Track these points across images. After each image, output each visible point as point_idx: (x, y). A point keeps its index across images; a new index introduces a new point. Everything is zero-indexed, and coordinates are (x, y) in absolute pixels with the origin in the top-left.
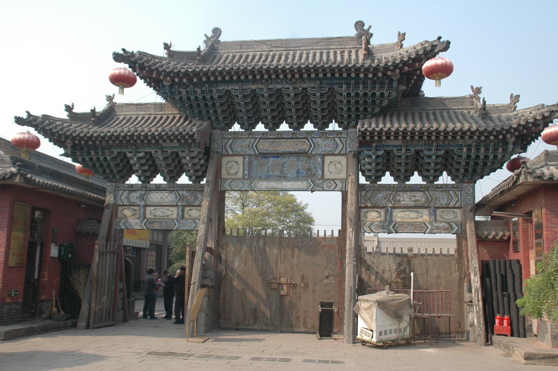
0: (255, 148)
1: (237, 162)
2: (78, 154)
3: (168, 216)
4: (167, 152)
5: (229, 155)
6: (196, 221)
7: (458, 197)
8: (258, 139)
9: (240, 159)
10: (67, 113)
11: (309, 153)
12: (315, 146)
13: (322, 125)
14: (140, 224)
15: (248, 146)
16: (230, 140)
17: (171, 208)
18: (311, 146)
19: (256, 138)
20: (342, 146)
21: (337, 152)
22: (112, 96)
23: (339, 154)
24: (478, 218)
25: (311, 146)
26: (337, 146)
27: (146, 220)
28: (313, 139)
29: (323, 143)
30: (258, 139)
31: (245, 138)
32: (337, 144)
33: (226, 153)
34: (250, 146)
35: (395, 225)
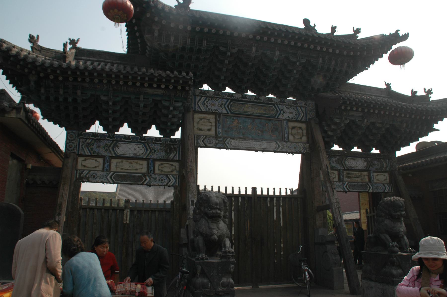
0: (227, 108)
1: (209, 120)
2: (43, 90)
3: (136, 170)
4: (148, 99)
5: (201, 112)
6: (168, 176)
8: (230, 100)
9: (212, 118)
10: (31, 44)
11: (276, 117)
13: (282, 95)
15: (221, 106)
16: (203, 98)
17: (141, 162)
18: (277, 112)
19: (228, 99)
20: (303, 114)
22: (76, 40)
23: (301, 122)
25: (277, 112)
26: (299, 114)
27: (112, 173)
29: (288, 111)
30: (230, 100)
31: (218, 98)
32: (298, 112)
33: (199, 110)
34: (223, 106)
35: (347, 185)
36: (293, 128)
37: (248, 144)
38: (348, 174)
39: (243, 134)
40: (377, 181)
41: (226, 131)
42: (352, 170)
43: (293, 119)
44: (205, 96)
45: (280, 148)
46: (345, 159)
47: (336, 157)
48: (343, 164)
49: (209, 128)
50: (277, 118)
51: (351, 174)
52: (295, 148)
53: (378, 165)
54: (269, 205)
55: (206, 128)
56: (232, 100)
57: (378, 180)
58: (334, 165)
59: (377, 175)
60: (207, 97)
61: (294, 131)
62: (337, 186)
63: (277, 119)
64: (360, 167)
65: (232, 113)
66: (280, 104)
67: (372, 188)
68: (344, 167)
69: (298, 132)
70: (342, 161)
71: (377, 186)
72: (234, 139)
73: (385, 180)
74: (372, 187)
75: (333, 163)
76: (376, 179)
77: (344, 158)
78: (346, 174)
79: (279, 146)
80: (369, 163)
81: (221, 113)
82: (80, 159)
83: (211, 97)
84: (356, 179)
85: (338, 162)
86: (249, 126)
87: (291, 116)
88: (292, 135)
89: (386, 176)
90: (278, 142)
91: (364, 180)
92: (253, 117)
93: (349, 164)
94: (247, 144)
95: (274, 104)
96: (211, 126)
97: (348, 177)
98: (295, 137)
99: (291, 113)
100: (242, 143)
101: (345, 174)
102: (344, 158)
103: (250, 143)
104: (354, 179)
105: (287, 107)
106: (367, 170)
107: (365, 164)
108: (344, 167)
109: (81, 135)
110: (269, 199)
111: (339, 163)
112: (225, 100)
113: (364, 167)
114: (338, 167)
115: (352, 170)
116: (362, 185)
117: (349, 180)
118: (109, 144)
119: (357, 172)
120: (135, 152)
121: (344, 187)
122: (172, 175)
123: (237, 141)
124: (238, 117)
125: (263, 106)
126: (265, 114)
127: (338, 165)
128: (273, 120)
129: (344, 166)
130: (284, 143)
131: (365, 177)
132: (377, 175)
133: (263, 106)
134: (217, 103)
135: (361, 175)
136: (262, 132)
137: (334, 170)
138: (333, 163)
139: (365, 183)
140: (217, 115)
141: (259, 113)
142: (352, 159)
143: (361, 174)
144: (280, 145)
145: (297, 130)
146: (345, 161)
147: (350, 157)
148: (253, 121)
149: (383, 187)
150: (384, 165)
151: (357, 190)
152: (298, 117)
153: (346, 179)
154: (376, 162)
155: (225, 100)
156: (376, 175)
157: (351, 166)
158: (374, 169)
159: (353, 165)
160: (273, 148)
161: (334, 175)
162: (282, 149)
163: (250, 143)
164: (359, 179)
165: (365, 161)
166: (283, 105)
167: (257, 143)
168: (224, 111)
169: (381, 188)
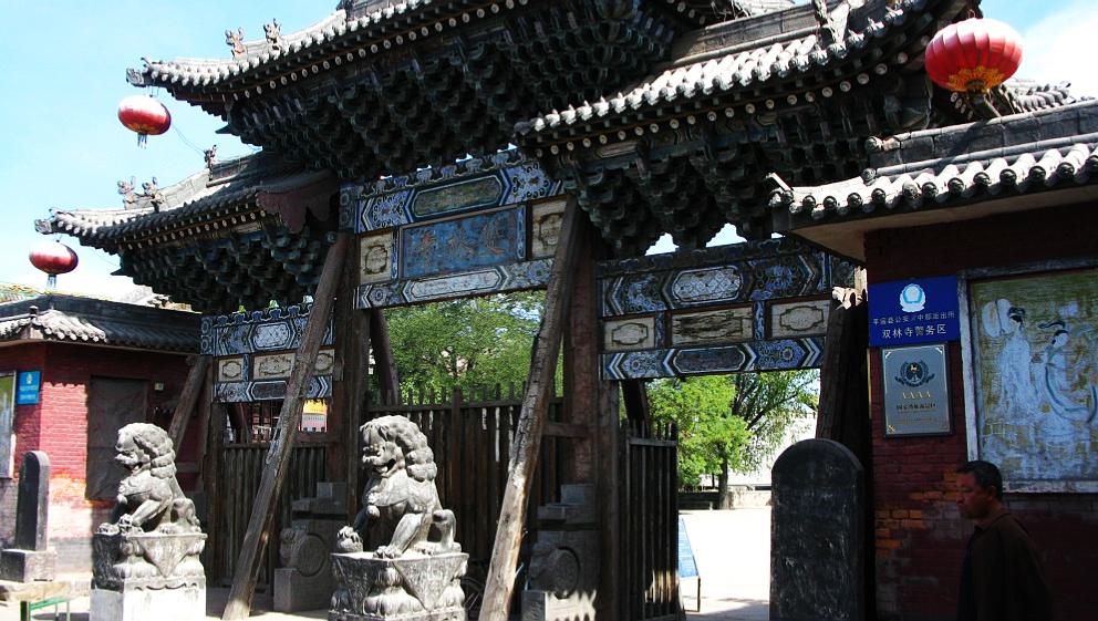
7: (820, 270)
9: (387, 239)
12: (511, 186)
14: (657, 364)
15: (398, 210)
18: (504, 187)
19: (411, 189)
21: (553, 193)
24: (29, 382)
25: (504, 187)
28: (508, 171)
35: (674, 354)
36: (545, 218)
37: (443, 286)
38: (687, 321)
39: (439, 264)
40: (786, 333)
41: (409, 265)
42: (692, 309)
43: (540, 197)
44: (372, 197)
45: (506, 282)
46: (673, 279)
47: (644, 279)
48: (666, 295)
49: (382, 264)
50: (504, 205)
51: (696, 320)
52: (539, 273)
53: (785, 277)
54: (485, 427)
55: (379, 265)
56: (418, 189)
57: (789, 328)
58: (638, 301)
59: (788, 311)
60: (376, 197)
61: (547, 227)
62: (645, 364)
63: (503, 208)
64: (720, 295)
65: (416, 220)
66: (510, 167)
67: (754, 357)
68: (667, 304)
69: (554, 229)
70: (661, 287)
71: (776, 351)
72: (417, 280)
73: (815, 325)
74: (756, 353)
75: (635, 296)
76: (782, 326)
77: (670, 278)
78: (678, 323)
79: (504, 277)
80: (751, 277)
81: (399, 226)
82: (222, 363)
83: (381, 195)
84: (711, 334)
85: (648, 292)
86: (450, 242)
87: (533, 189)
88: (541, 239)
89: (821, 310)
90: (502, 268)
91: (739, 334)
92: (457, 216)
93: (683, 293)
94: (439, 286)
95: (496, 172)
96: (386, 258)
97: (685, 332)
98: (545, 244)
99: (535, 181)
100: (431, 285)
101: (675, 323)
102: (670, 278)
103: (445, 283)
104: (705, 334)
105: (526, 167)
106: (742, 299)
107: (737, 282)
108: (667, 304)
109: (215, 322)
110: (484, 412)
111: (651, 293)
112: (406, 193)
113: (734, 293)
114: (650, 306)
115: (692, 309)
116: (719, 353)
117: (688, 339)
118: (247, 331)
119: (716, 312)
120: (277, 339)
121: (665, 363)
122: (324, 376)
123: (422, 284)
124: (428, 225)
125: (474, 184)
126: (477, 203)
127: (650, 299)
128: (495, 213)
129: (669, 299)
130: (516, 266)
131: (741, 324)
132: (788, 311)
133: (474, 184)
134: (391, 205)
135: (729, 319)
136: (476, 249)
137: (641, 317)
138: (635, 296)
139: (733, 344)
140: (395, 230)
141: (467, 205)
142: (694, 273)
143: (730, 317)
144: (506, 273)
145: (553, 222)
146: (671, 284)
147: (686, 269)
148: (459, 226)
149: (798, 349)
150: (808, 274)
151: (705, 369)
152: (550, 189)
153: (677, 339)
154: (777, 271)
155: (406, 193)
156: (784, 311)
157: (690, 295)
158: (768, 294)
159: (697, 294)
160: (493, 284)
161: (645, 330)
162: (510, 284)
163: (445, 283)
164: (722, 332)
165: (735, 272)
166: (517, 165)
167: (460, 279)
168: (404, 220)
169: (788, 354)
